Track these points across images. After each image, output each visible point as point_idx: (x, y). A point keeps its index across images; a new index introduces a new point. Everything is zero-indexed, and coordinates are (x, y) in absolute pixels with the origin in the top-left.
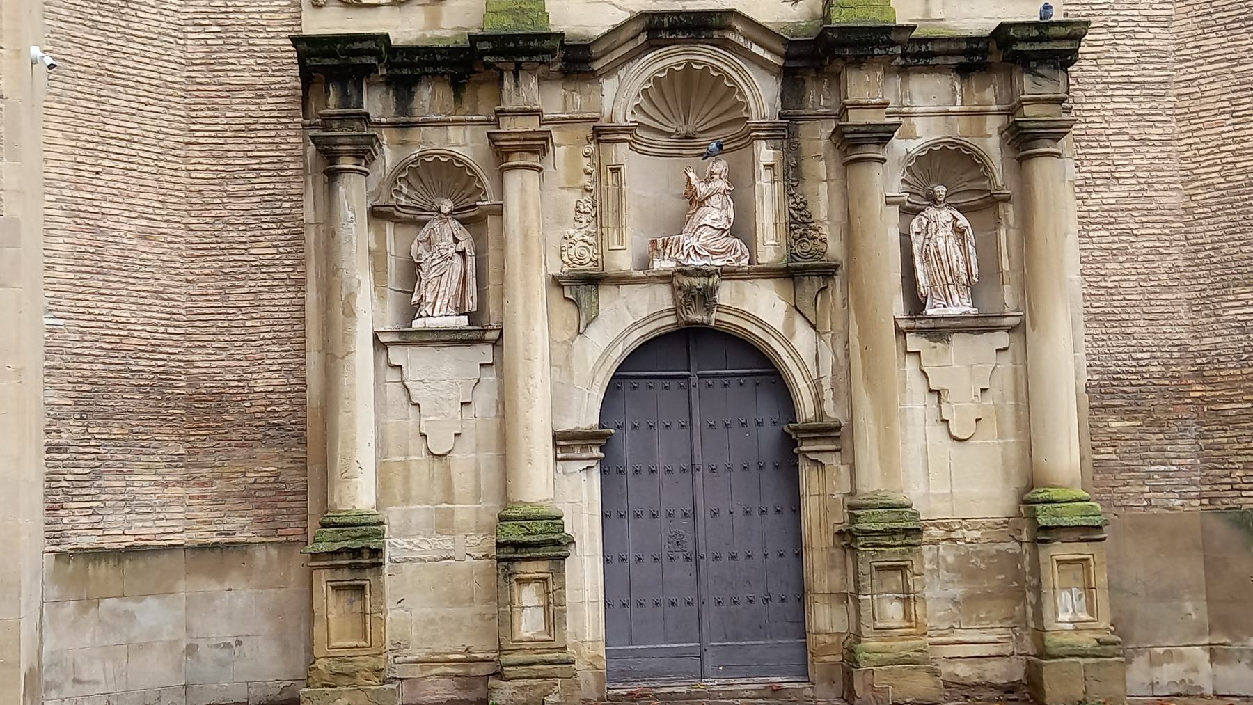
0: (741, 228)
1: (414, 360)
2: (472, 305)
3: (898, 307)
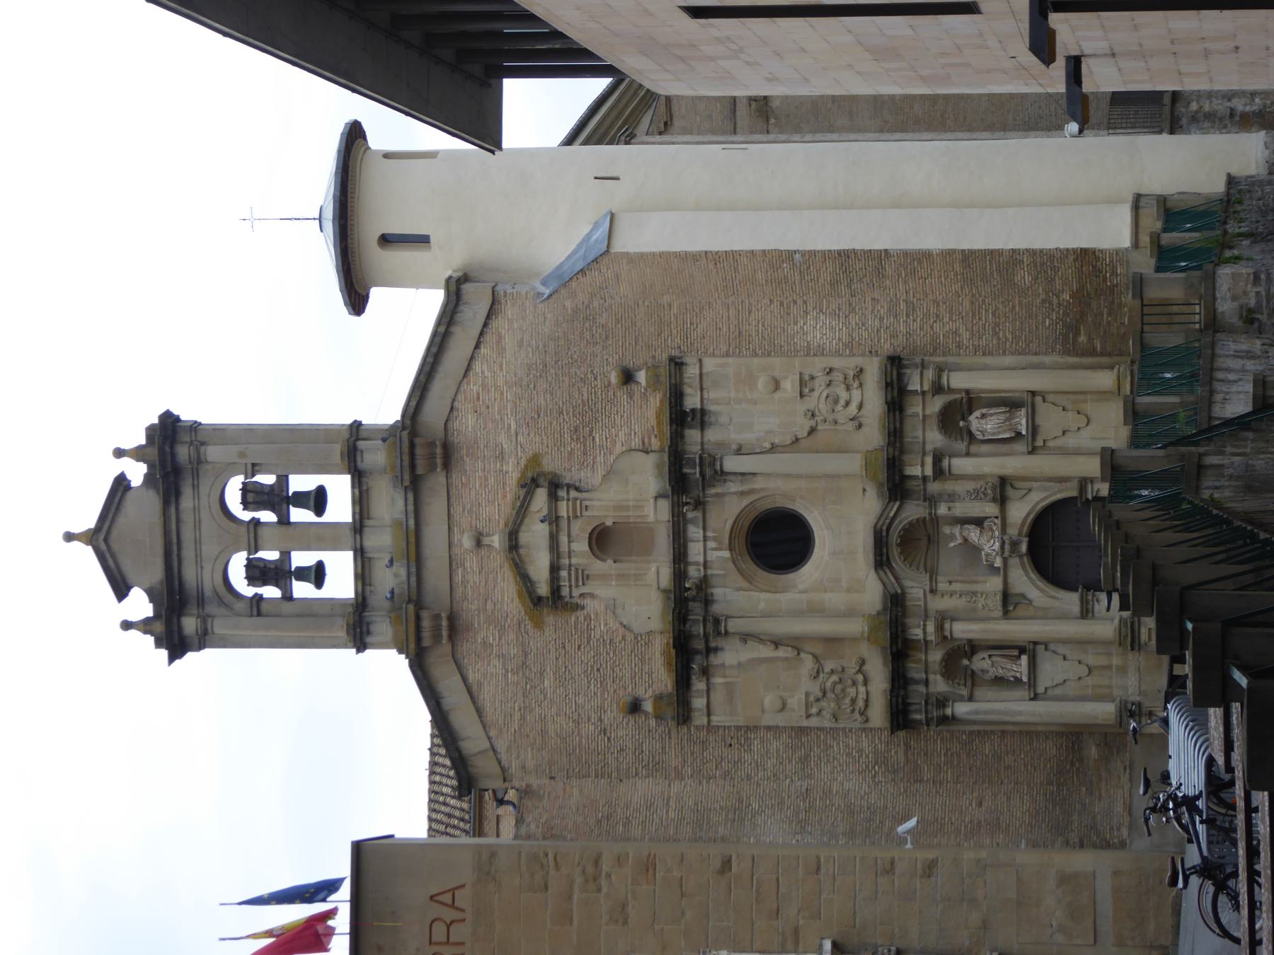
0: (979, 522)
1: (1043, 683)
2: (1016, 653)
3: (1020, 447)
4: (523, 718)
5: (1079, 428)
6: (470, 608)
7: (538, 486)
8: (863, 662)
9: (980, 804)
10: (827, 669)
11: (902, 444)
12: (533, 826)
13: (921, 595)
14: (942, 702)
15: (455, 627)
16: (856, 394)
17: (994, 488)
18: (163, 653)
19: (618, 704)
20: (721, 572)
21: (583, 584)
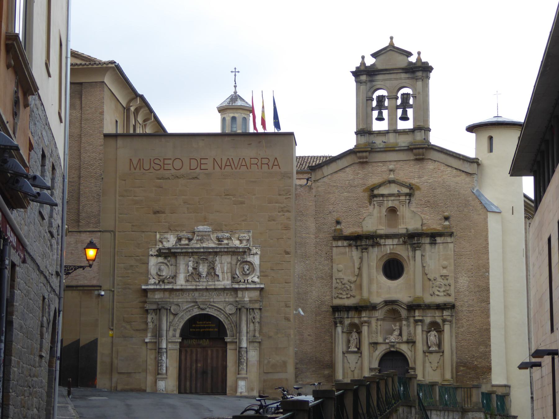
0: (400, 334)
1: (349, 356)
3: (425, 348)
4: (334, 186)
5: (432, 367)
6: (369, 169)
7: (410, 189)
8: (354, 297)
9: (309, 335)
10: (351, 285)
11: (426, 309)
12: (299, 190)
13: (376, 316)
14: (341, 323)
15: (363, 164)
16: (442, 294)
17: (411, 339)
18: (354, 70)
19: (339, 217)
20: (382, 250)
21: (378, 205)
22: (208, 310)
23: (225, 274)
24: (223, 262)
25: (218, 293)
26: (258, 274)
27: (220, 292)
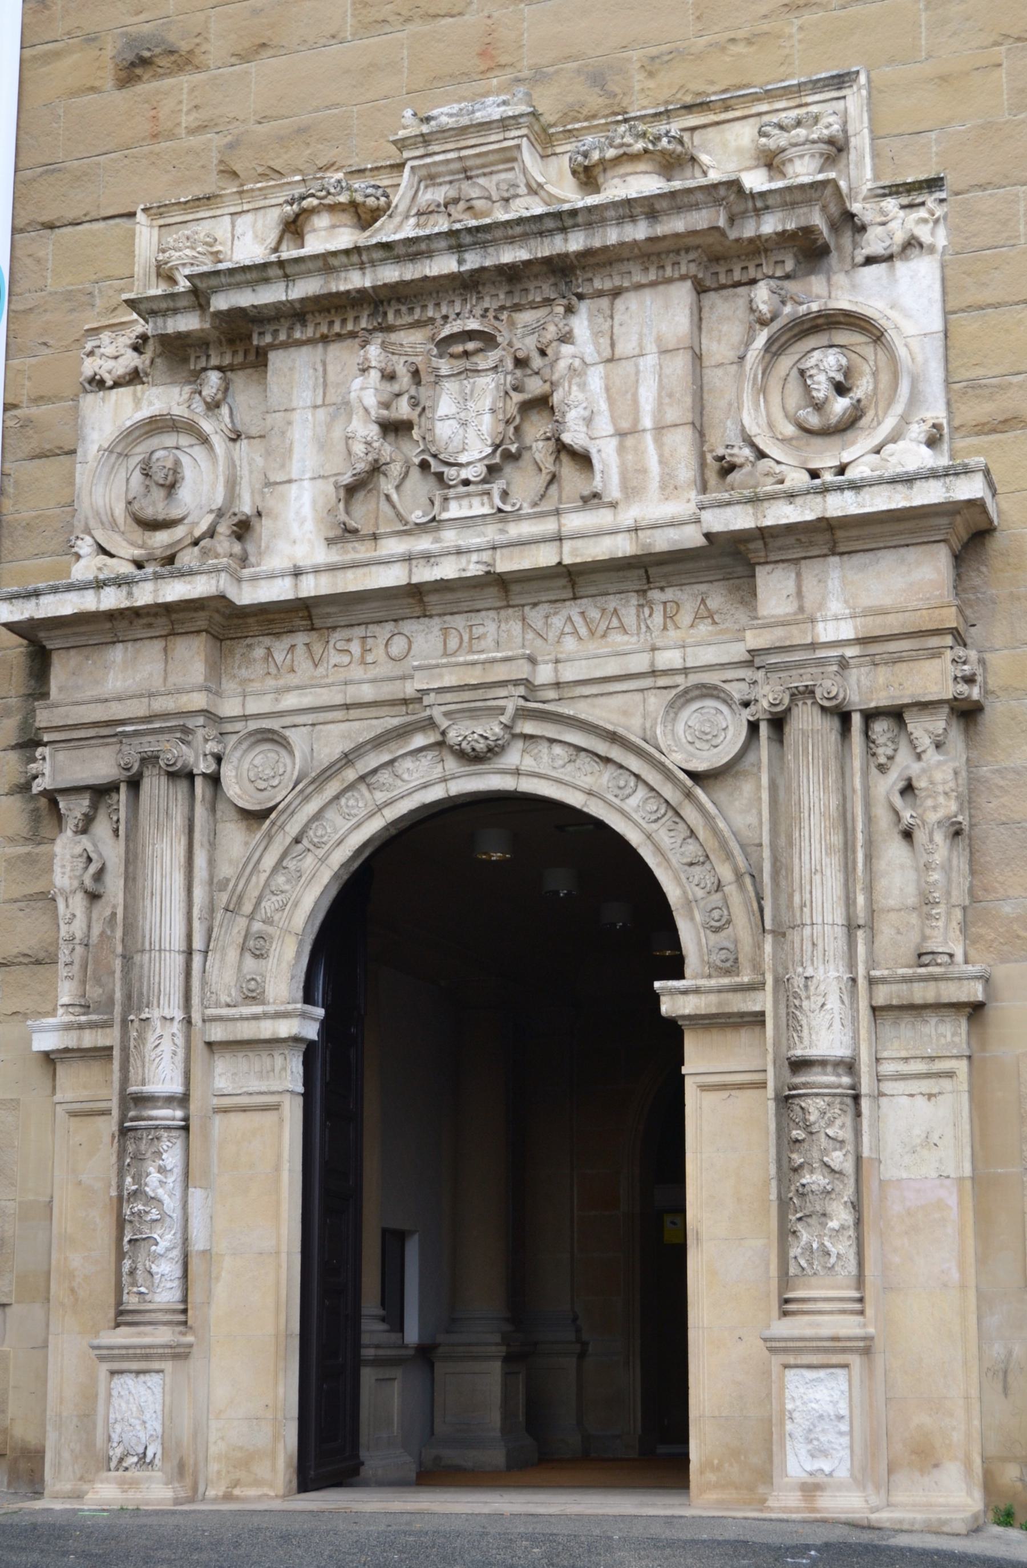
22: (513, 757)
23: (649, 438)
24: (626, 346)
25: (594, 614)
26: (936, 411)
27: (612, 602)
